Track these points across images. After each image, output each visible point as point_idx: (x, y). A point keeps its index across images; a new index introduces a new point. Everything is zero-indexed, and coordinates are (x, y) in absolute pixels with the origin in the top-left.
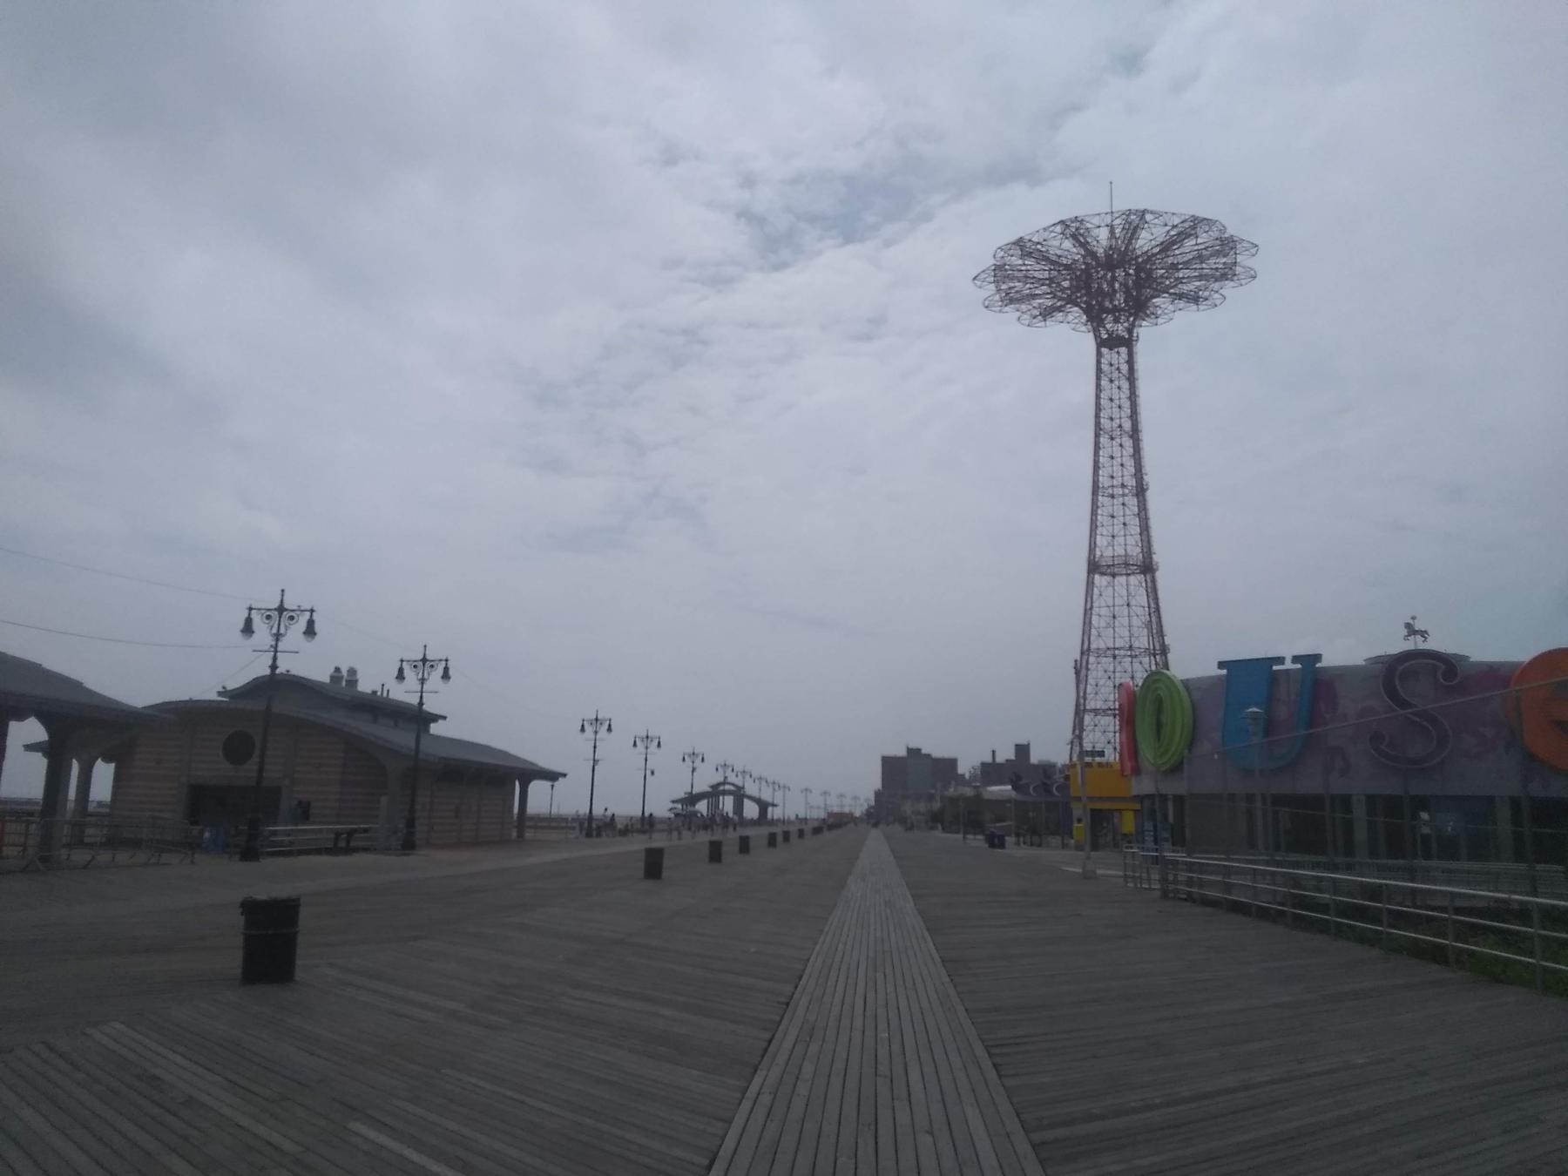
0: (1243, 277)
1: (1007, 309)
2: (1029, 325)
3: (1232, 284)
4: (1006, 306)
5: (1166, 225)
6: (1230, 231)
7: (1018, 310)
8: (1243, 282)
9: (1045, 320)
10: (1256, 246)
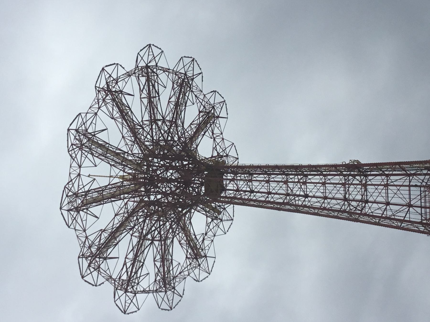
0: (191, 69)
1: (179, 288)
2: (209, 274)
3: (198, 80)
4: (174, 288)
5: (96, 114)
6: (130, 66)
7: (185, 278)
8: (197, 71)
9: (206, 256)
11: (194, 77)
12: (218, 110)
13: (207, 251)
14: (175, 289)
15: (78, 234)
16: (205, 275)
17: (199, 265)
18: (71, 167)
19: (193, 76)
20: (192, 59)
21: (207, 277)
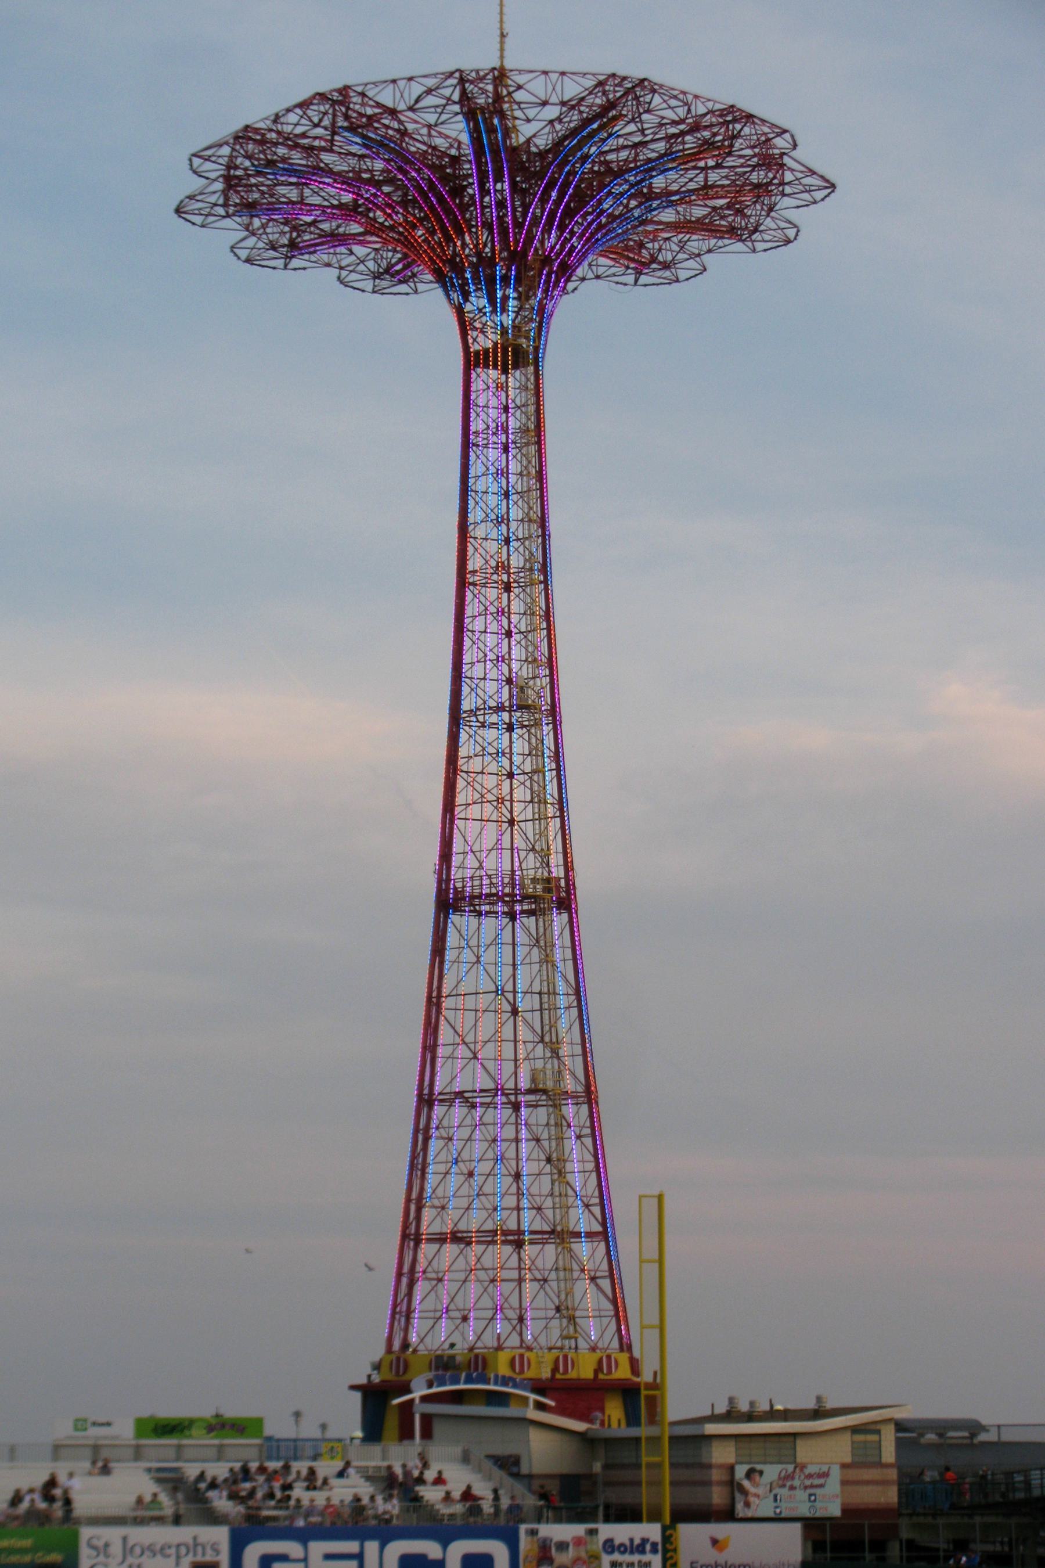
4: (228, 216)
8: (760, 246)
10: (833, 186)
11: (749, 244)
12: (659, 273)
13: (306, 257)
14: (224, 217)
15: (402, 84)
16: (243, 254)
17: (273, 248)
18: (563, 74)
19: (753, 241)
20: (792, 238)
21: (239, 258)
